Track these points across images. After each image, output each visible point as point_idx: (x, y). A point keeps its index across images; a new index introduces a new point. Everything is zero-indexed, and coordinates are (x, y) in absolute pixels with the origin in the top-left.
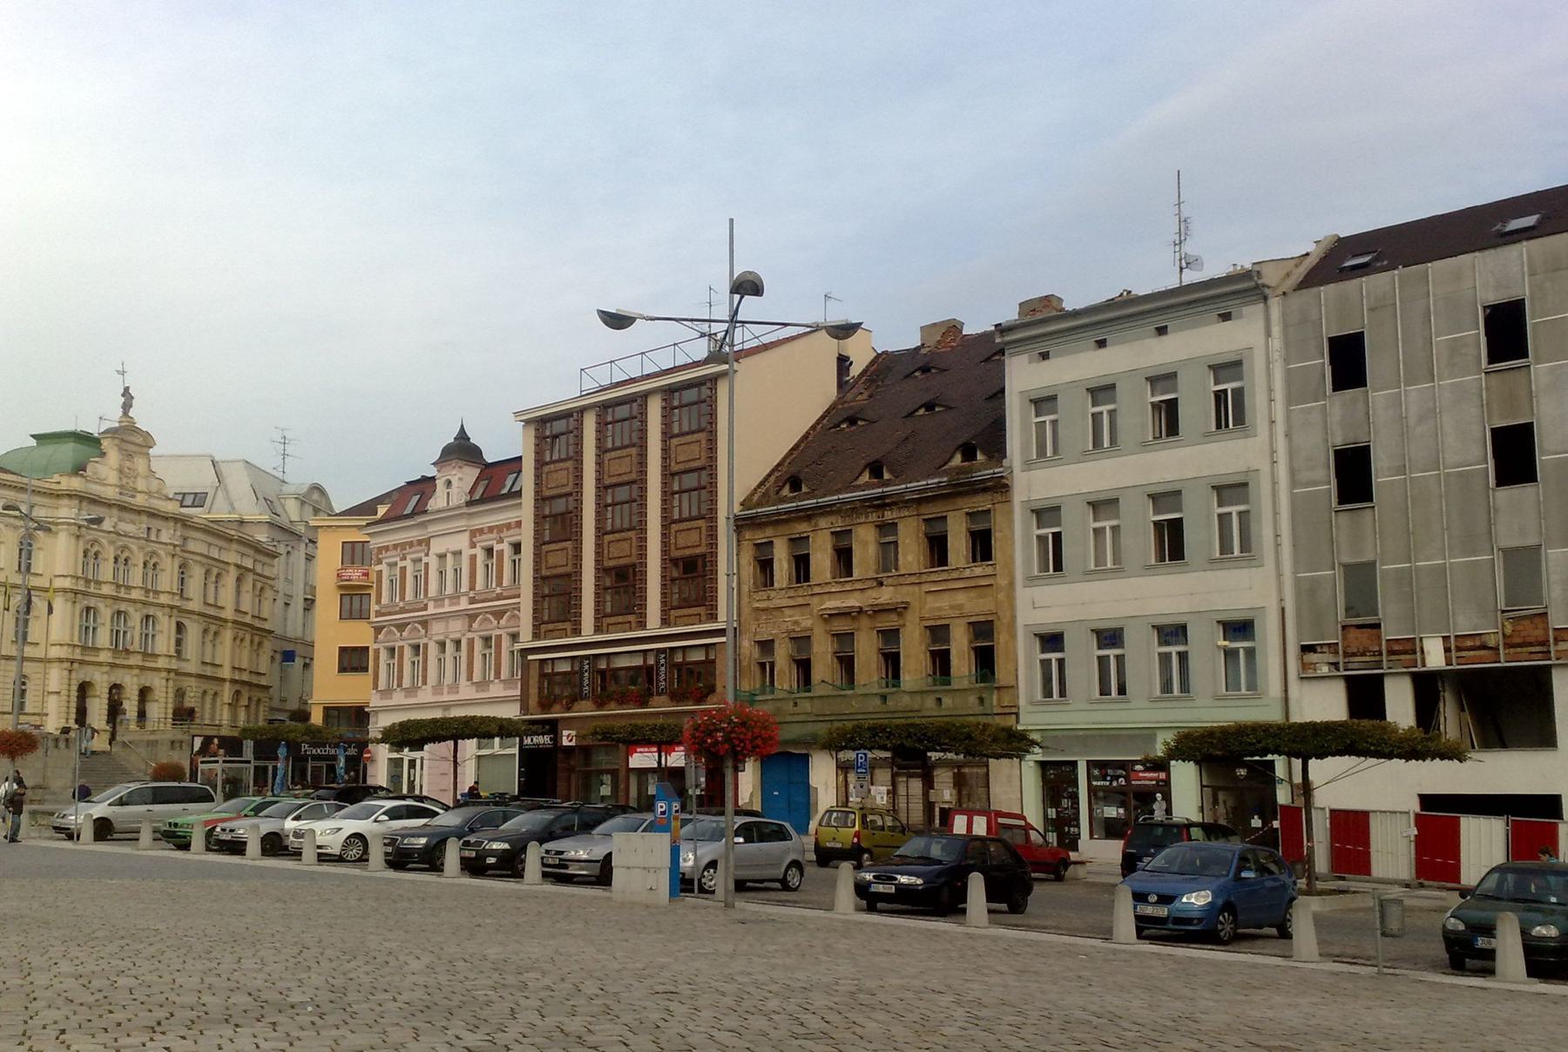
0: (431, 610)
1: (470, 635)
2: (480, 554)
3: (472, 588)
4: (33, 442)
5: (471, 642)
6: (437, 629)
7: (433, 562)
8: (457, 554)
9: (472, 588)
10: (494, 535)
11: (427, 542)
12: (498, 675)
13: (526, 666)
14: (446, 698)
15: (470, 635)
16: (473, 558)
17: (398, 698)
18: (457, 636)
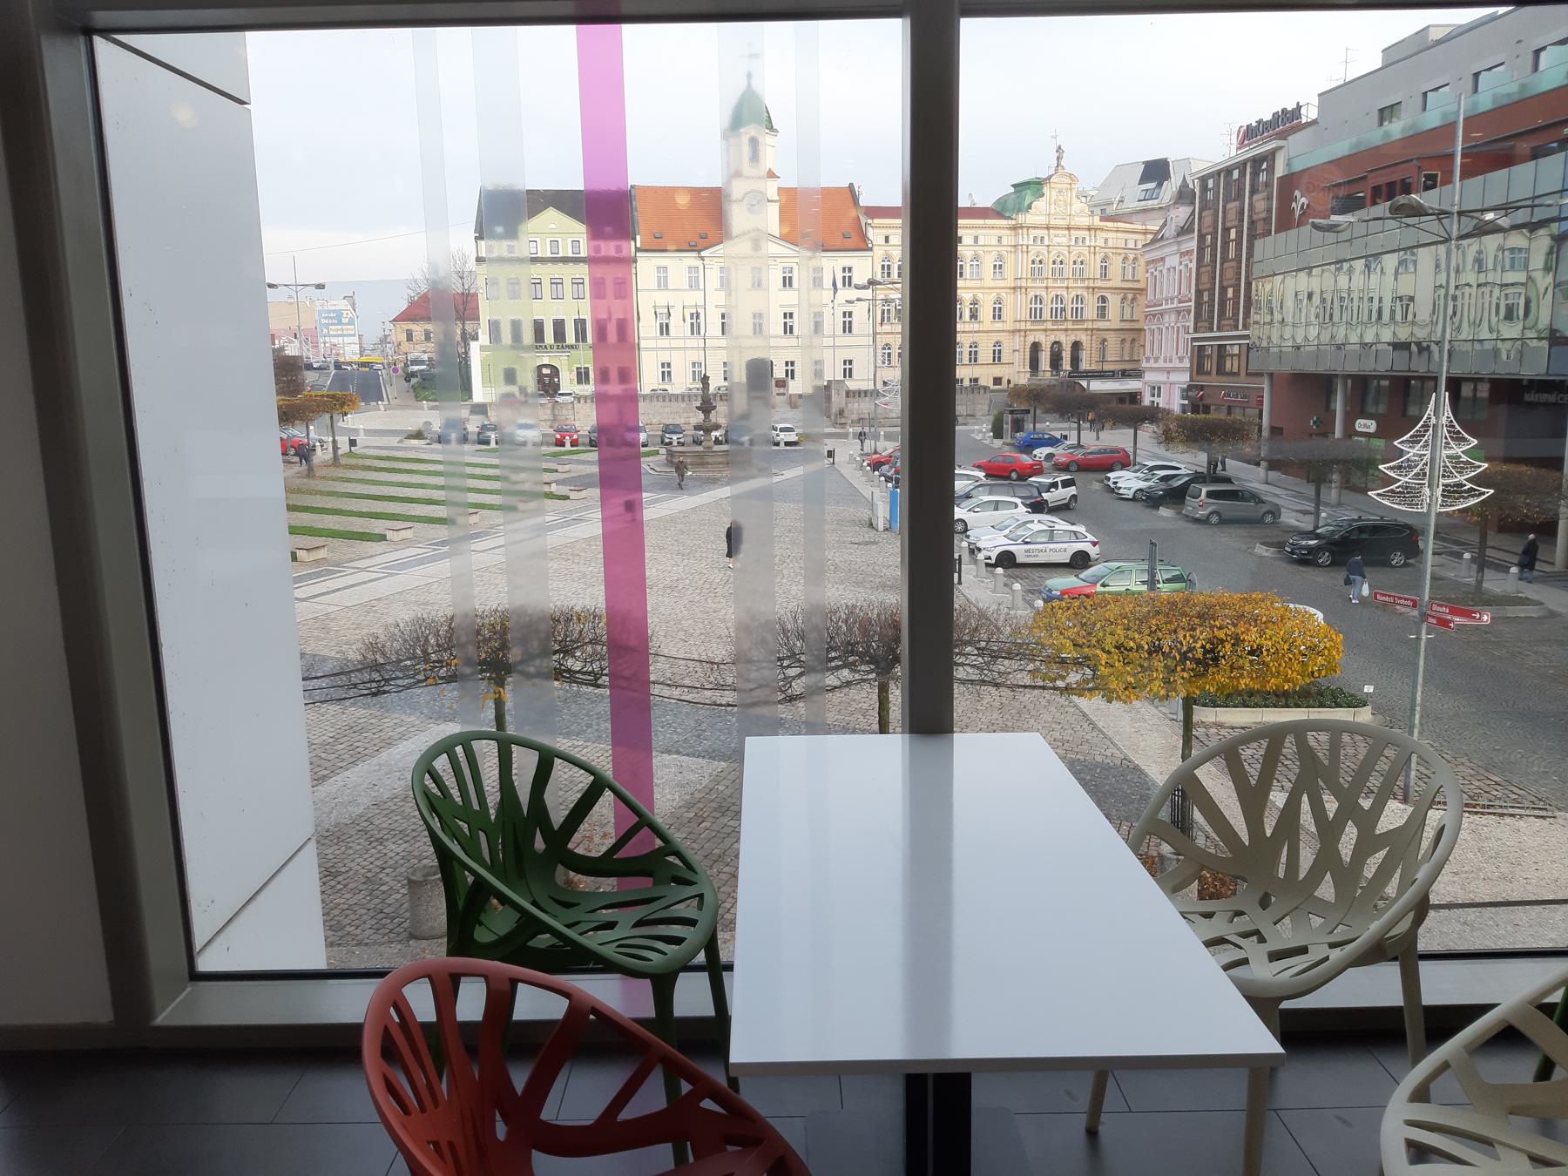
0: (1164, 307)
1: (1178, 325)
2: (1182, 267)
3: (1180, 293)
4: (1012, 190)
5: (1178, 327)
6: (1166, 318)
7: (1165, 272)
8: (1175, 268)
9: (1180, 293)
10: (1187, 257)
11: (1163, 259)
12: (1187, 354)
13: (1193, 347)
14: (1168, 365)
15: (1178, 325)
16: (1181, 271)
17: (1152, 364)
18: (1173, 324)
